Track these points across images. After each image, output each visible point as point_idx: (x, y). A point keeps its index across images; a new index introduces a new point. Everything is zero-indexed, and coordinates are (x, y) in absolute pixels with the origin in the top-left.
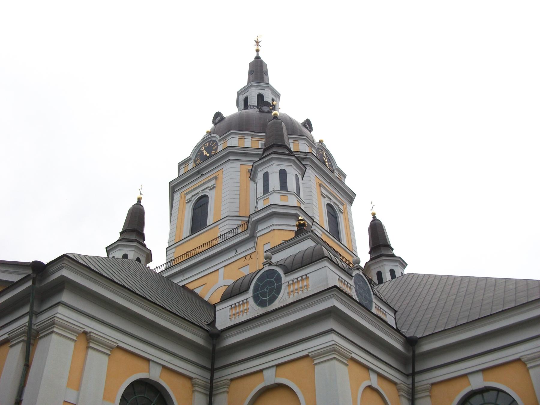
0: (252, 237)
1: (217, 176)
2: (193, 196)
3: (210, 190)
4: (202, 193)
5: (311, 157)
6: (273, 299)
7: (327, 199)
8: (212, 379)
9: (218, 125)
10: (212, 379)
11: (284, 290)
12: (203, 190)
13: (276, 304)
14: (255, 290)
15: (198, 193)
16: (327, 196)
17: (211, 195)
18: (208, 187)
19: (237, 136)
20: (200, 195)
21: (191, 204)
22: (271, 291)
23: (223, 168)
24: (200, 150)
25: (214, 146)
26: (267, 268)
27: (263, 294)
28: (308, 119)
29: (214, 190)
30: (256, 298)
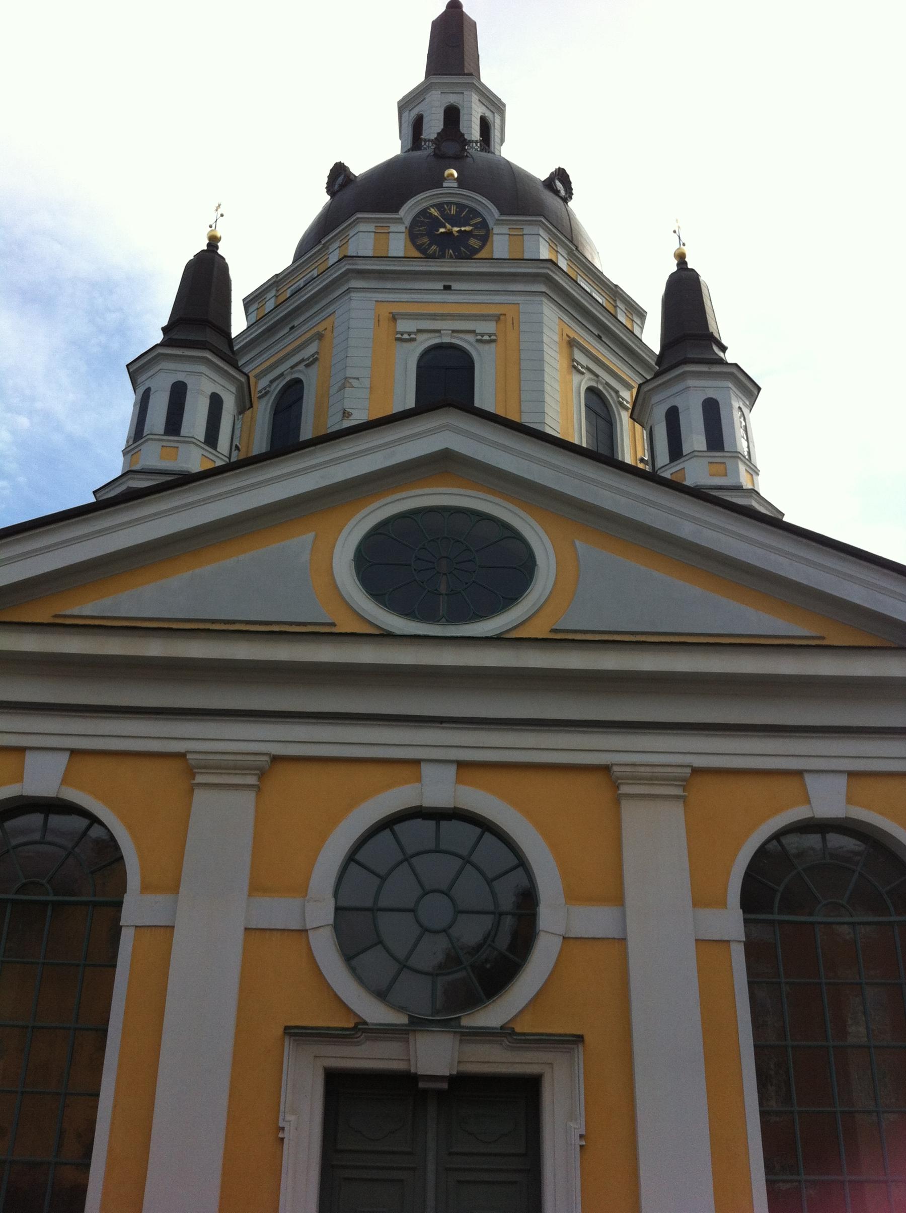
1: (323, 333)
2: (272, 382)
3: (307, 366)
4: (292, 374)
7: (588, 375)
9: (339, 195)
12: (292, 367)
15: (282, 375)
16: (588, 369)
17: (311, 380)
18: (303, 360)
19: (371, 227)
20: (288, 379)
21: (268, 402)
23: (335, 312)
28: (559, 168)
29: (315, 367)
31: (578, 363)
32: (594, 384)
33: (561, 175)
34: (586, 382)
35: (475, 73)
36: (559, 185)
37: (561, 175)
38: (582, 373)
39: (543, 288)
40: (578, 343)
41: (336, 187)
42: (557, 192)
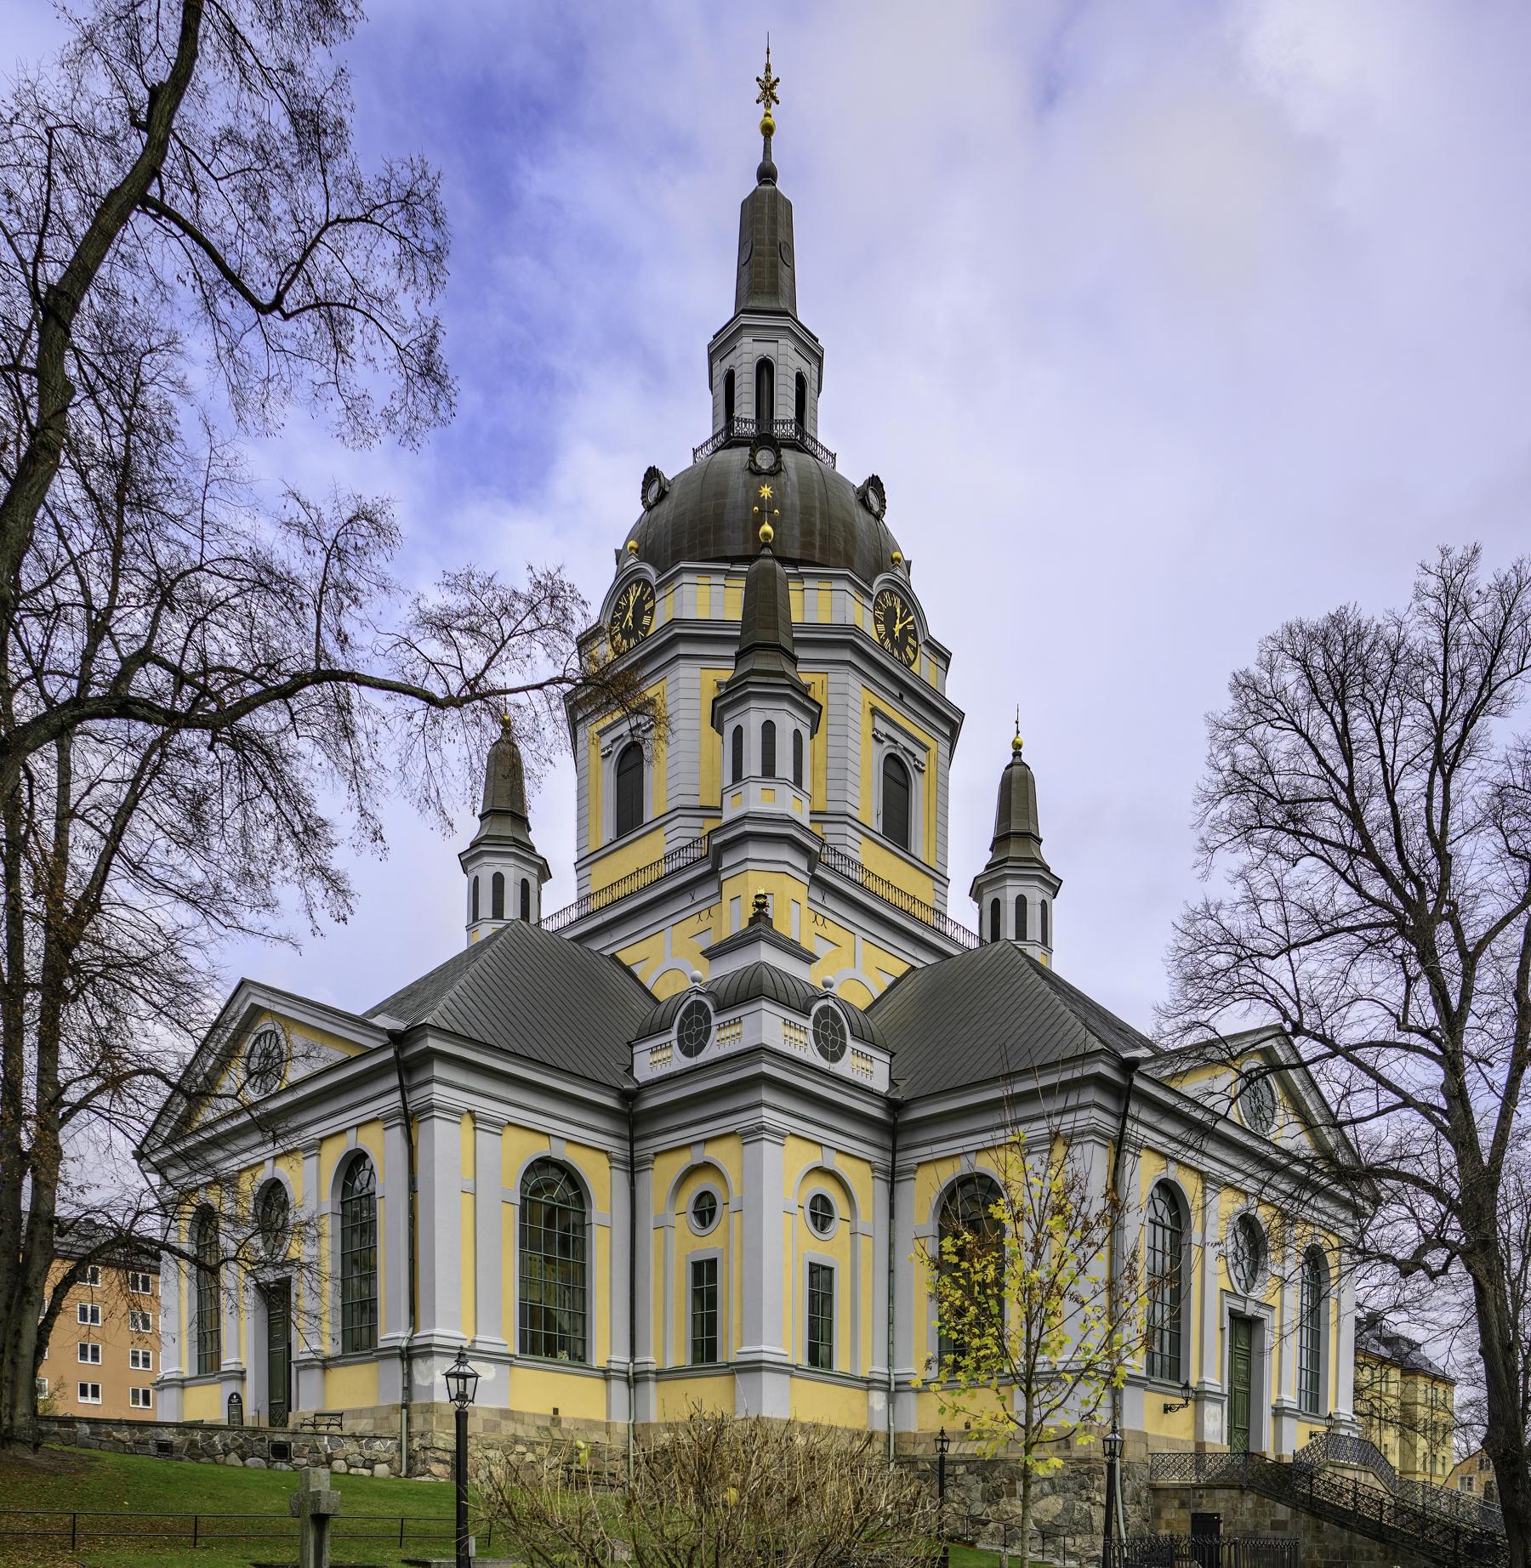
0: (713, 875)
5: (852, 637)
6: (700, 1048)
8: (632, 1152)
9: (656, 510)
10: (632, 1152)
11: (715, 1035)
13: (703, 1057)
14: (680, 1030)
22: (699, 1033)
24: (618, 604)
25: (647, 601)
26: (694, 998)
27: (689, 1037)
30: (680, 1040)
31: (878, 732)
32: (893, 751)
33: (875, 483)
34: (886, 748)
35: (788, 313)
36: (873, 498)
37: (875, 483)
38: (882, 742)
39: (847, 655)
40: (879, 711)
41: (651, 500)
42: (869, 509)
